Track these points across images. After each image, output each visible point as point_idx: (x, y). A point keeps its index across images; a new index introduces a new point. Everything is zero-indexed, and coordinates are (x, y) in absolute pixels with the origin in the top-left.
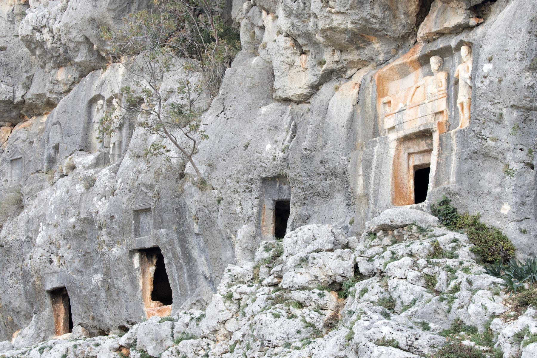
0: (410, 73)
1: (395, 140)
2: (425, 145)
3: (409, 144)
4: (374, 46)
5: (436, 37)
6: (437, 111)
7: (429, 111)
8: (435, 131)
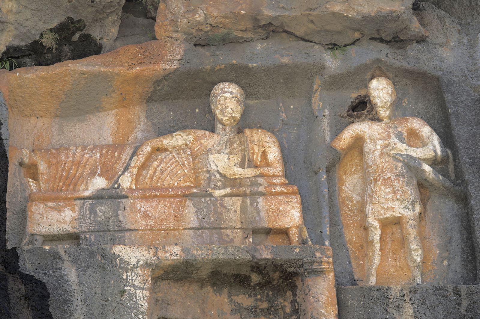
0: (98, 109)
1: (147, 265)
2: (227, 308)
3: (172, 290)
5: (249, 35)
6: (264, 224)
7: (234, 218)
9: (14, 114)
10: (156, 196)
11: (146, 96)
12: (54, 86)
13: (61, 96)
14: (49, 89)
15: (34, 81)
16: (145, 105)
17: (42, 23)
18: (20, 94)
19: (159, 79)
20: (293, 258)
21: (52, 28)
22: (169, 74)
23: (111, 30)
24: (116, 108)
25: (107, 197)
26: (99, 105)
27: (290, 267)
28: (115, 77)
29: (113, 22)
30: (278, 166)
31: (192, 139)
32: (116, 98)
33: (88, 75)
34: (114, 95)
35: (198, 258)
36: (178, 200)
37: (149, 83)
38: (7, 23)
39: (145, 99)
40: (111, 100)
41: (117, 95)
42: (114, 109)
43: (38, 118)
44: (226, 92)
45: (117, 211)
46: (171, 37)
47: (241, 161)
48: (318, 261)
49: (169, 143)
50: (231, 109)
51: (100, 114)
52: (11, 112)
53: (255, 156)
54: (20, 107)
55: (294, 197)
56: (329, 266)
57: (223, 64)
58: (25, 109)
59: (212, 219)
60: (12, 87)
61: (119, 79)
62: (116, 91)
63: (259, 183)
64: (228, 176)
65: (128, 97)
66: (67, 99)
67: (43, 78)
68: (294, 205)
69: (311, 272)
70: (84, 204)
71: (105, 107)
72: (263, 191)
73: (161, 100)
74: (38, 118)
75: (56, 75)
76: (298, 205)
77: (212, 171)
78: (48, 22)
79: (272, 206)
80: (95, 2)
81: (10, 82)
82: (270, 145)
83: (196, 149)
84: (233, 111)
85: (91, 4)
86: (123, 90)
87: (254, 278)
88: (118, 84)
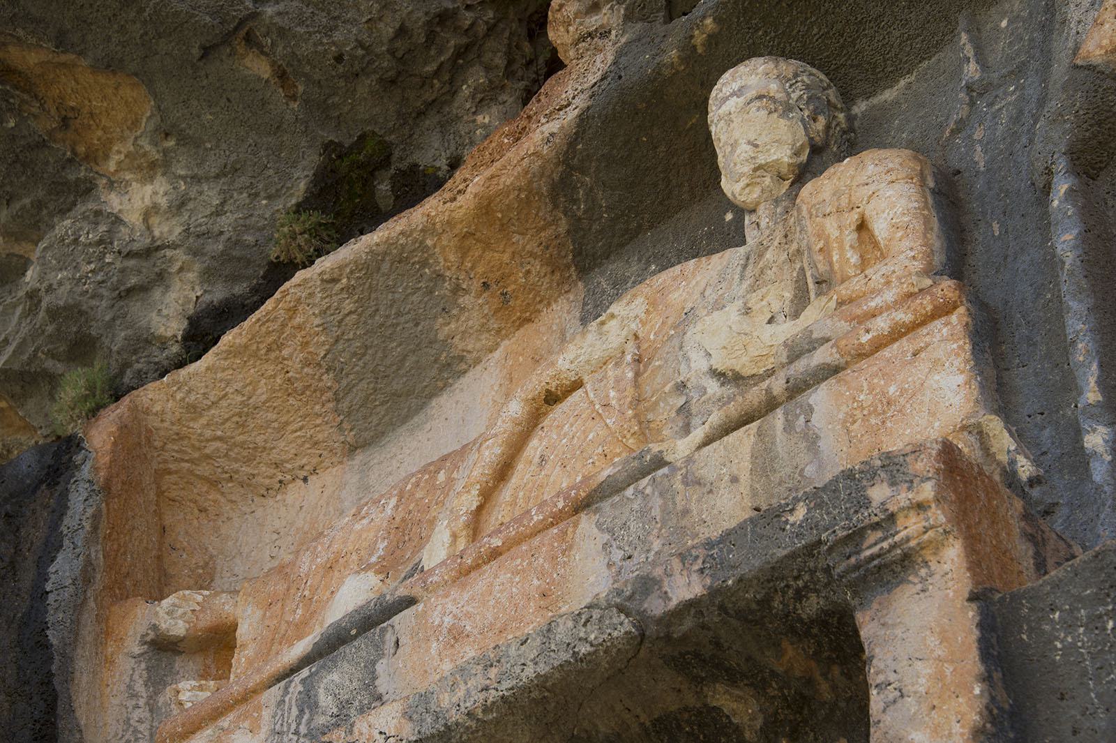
0: (451, 368)
4: (114, 202)
8: (897, 568)
9: (232, 502)
10: (495, 554)
11: (563, 253)
12: (284, 359)
13: (320, 380)
14: (274, 376)
15: (219, 375)
16: (580, 283)
17: (264, 202)
18: (208, 433)
19: (556, 177)
20: (785, 552)
21: (300, 199)
22: (572, 144)
23: (474, 121)
24: (502, 340)
25: (353, 632)
26: (444, 354)
27: (800, 595)
28: (429, 242)
29: (479, 96)
30: (906, 243)
31: (644, 308)
32: (481, 306)
33: (348, 278)
34: (465, 300)
35: (454, 716)
36: (556, 531)
37: (539, 209)
38: (158, 248)
39: (568, 267)
40: (468, 319)
41: (478, 296)
42: (498, 344)
43: (305, 480)
44: (727, 98)
45: (374, 663)
46: (590, 35)
47: (795, 296)
48: (876, 519)
49: (576, 358)
50: (749, 143)
51: (465, 380)
52: (223, 500)
53: (834, 253)
54: (237, 472)
55: (938, 323)
56: (927, 520)
57: (704, 17)
58: (256, 472)
59: (657, 545)
60: (173, 424)
61: (445, 243)
62: (464, 287)
63: (817, 340)
64: (747, 372)
65: (513, 287)
66: (344, 382)
67: (233, 352)
68: (940, 353)
69: (864, 579)
70: (286, 688)
71: (469, 352)
72: (829, 360)
73: (622, 245)
74: (305, 480)
75: (264, 324)
76: (955, 346)
77: (693, 378)
78: (277, 190)
79: (862, 397)
80: (346, 58)
81: (154, 410)
82: (872, 188)
83: (652, 337)
84: (756, 146)
85: (341, 69)
86: (480, 269)
87: (735, 705)
88: (452, 258)
